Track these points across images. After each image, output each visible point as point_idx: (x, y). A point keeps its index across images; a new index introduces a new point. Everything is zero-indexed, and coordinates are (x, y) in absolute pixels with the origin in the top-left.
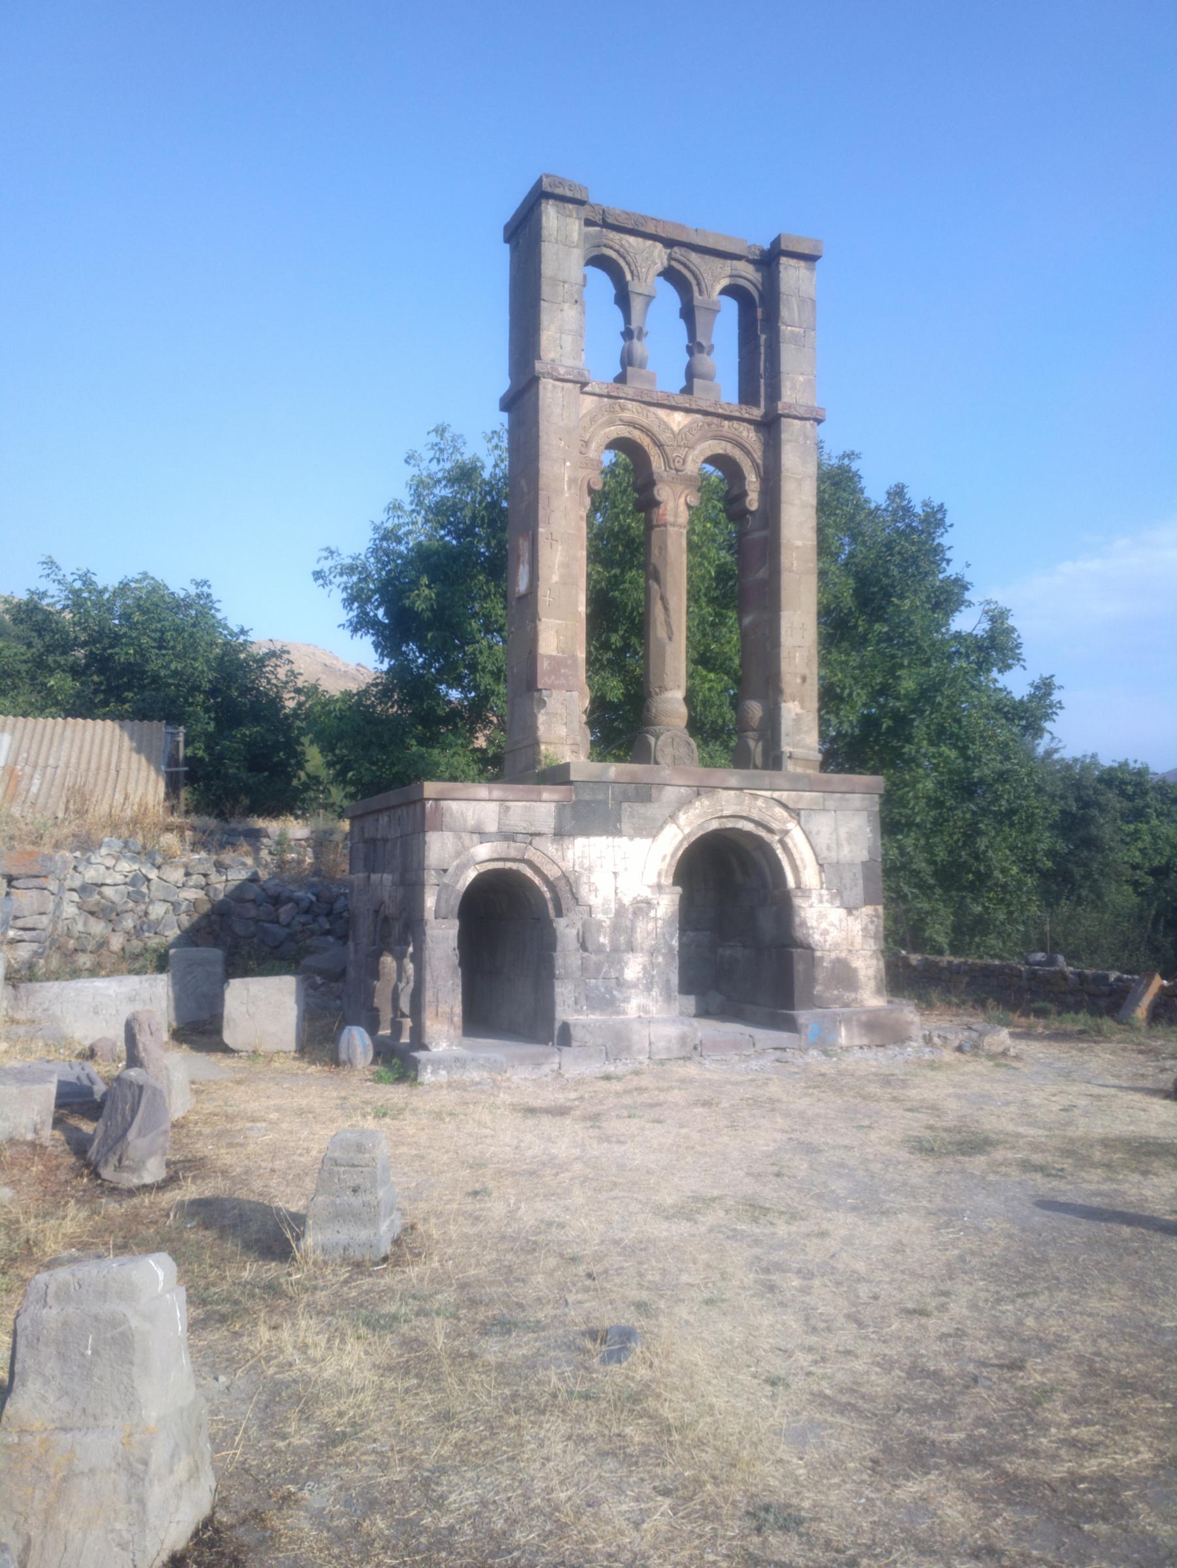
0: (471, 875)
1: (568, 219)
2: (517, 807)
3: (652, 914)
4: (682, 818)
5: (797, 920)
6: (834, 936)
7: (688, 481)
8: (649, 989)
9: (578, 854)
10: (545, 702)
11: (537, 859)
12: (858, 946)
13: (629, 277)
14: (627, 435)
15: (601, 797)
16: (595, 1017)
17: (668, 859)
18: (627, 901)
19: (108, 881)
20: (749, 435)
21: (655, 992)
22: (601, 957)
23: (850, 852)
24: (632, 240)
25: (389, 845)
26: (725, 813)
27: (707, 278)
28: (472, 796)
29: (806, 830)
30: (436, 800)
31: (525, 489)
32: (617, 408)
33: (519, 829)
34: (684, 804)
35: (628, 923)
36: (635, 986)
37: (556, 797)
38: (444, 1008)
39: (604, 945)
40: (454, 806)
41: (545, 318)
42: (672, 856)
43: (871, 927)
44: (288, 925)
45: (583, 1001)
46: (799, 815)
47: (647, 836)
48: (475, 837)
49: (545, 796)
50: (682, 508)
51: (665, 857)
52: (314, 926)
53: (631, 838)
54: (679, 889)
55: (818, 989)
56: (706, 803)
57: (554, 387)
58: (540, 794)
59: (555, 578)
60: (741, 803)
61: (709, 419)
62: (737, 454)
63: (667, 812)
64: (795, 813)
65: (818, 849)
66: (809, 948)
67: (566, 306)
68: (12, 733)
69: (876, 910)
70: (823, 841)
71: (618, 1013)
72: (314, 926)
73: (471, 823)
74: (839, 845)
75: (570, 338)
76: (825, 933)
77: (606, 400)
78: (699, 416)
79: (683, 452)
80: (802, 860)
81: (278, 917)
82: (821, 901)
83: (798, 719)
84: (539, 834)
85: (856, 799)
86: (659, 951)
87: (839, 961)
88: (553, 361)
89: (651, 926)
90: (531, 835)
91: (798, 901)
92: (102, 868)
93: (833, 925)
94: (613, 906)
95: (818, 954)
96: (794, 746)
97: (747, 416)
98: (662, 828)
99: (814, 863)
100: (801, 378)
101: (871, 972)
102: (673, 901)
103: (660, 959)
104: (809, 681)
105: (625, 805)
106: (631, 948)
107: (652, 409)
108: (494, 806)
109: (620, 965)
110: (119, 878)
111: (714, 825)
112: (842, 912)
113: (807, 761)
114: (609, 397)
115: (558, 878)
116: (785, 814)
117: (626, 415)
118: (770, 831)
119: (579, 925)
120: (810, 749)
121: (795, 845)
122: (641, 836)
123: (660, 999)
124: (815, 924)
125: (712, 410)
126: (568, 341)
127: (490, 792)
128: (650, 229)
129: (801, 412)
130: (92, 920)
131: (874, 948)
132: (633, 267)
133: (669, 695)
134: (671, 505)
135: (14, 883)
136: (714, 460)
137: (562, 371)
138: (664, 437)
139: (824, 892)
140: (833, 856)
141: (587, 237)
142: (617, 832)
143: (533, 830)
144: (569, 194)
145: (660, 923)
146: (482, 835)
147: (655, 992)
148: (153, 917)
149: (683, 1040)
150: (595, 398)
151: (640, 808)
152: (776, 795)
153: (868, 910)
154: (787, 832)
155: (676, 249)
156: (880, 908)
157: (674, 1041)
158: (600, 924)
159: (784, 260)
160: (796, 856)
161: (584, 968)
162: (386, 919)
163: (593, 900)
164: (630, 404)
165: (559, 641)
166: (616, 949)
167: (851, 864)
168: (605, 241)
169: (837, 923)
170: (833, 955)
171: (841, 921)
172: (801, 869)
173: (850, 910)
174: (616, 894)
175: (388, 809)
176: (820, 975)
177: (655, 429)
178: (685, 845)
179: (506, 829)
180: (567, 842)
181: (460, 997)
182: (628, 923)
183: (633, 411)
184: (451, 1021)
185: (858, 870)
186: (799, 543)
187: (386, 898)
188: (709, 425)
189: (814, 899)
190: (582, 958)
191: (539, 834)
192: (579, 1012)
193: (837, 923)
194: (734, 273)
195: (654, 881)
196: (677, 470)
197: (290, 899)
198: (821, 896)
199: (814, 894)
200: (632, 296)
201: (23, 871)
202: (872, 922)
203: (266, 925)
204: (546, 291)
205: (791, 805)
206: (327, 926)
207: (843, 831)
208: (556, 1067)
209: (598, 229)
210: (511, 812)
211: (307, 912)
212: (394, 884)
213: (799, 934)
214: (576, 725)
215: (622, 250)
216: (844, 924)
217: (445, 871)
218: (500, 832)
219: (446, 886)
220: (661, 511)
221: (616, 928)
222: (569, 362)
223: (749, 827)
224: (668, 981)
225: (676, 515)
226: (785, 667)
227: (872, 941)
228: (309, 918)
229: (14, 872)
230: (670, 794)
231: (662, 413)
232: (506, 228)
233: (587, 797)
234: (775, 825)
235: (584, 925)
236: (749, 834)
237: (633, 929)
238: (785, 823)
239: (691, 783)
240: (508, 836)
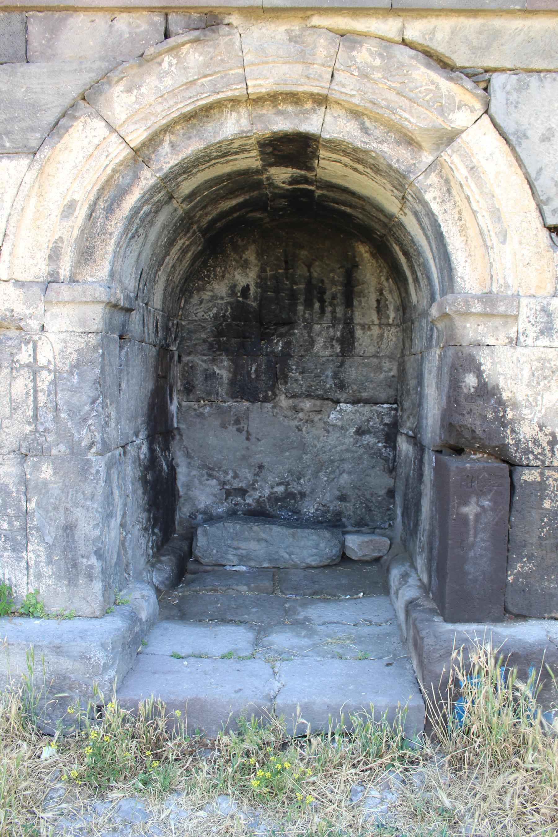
4: (120, 102)
17: (82, 212)
21: (35, 552)
26: (260, 85)
29: (509, 127)
51: (70, 208)
56: (194, 57)
60: (303, 57)
63: (72, 86)
80: (496, 214)
86: (43, 452)
89: (21, 385)
98: (56, 129)
99: (537, 223)
102: (83, 321)
103: (47, 472)
123: (48, 570)
145: (46, 378)
147: (35, 552)
152: (416, 30)
160: (480, 203)
172: (494, 241)
195: (39, 268)
199: (527, 310)
205: (460, 59)
224: (69, 529)
234: (416, 120)
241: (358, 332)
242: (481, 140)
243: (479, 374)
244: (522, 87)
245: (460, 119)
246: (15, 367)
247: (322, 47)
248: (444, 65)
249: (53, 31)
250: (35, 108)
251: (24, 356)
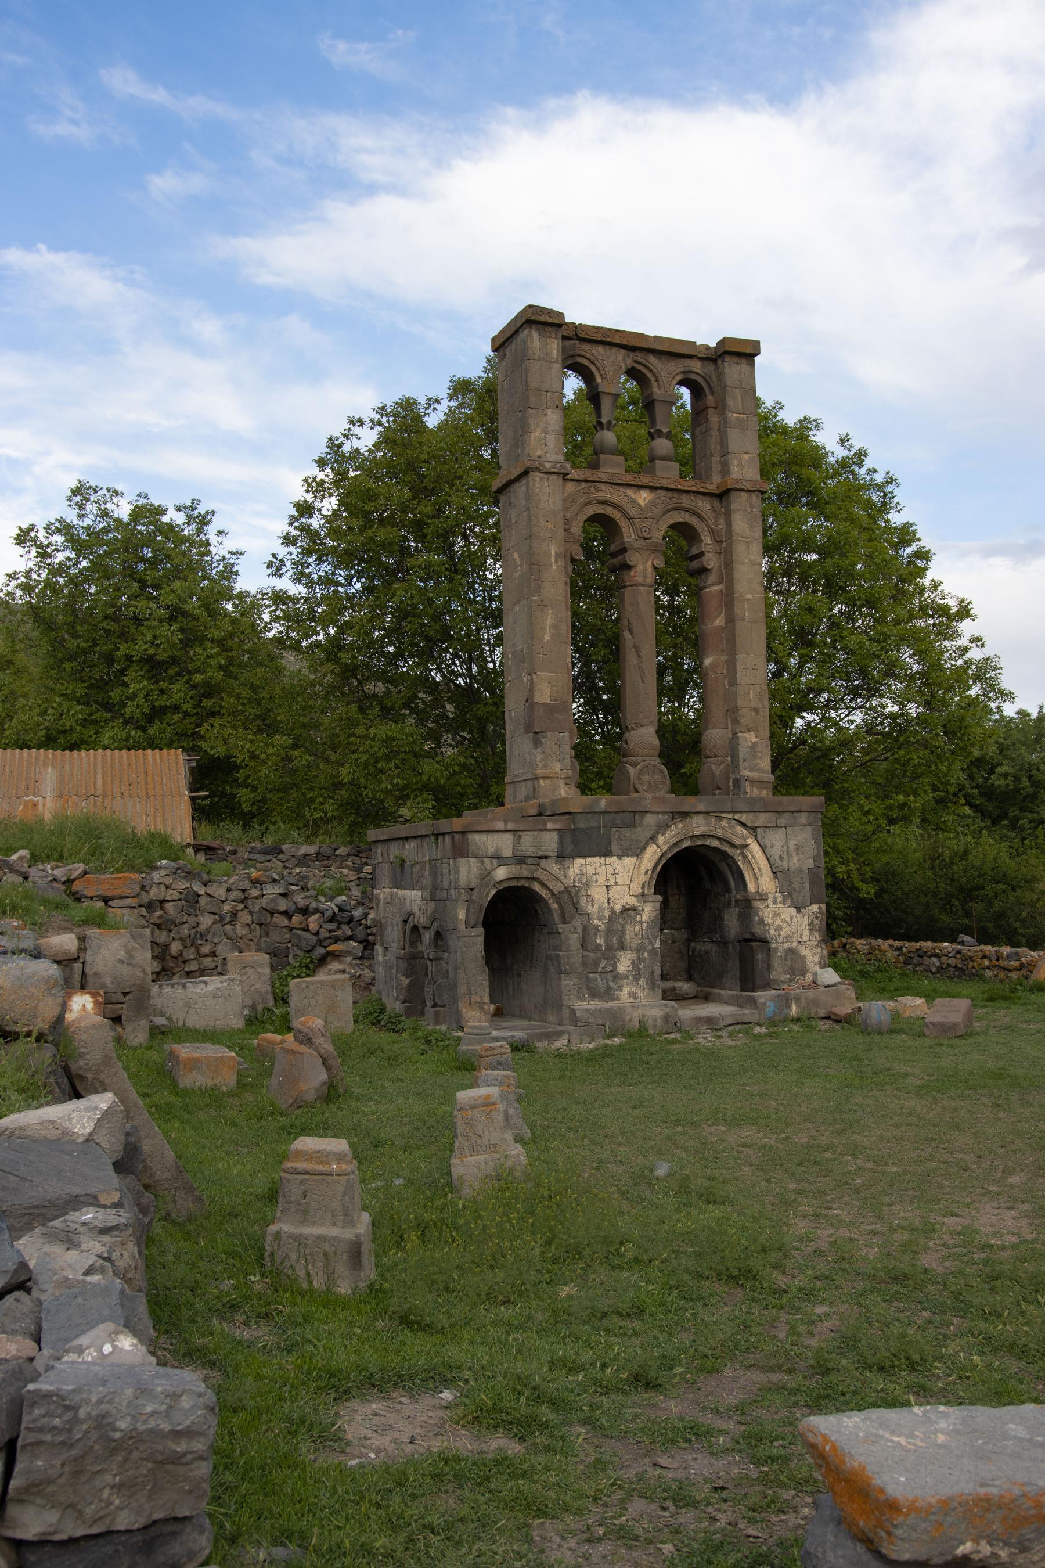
0: (493, 892)
1: (548, 340)
2: (527, 838)
3: (638, 919)
4: (661, 840)
5: (757, 918)
6: (786, 930)
7: (654, 549)
8: (637, 979)
9: (577, 871)
10: (541, 743)
11: (543, 878)
12: (805, 938)
13: (599, 380)
14: (602, 511)
15: (594, 824)
16: (595, 1004)
17: (650, 873)
18: (618, 908)
19: (168, 898)
20: (704, 505)
21: (642, 982)
22: (599, 955)
23: (799, 860)
24: (600, 349)
25: (417, 868)
26: (695, 833)
27: (664, 376)
28: (491, 829)
30: (463, 833)
31: (518, 562)
32: (593, 490)
33: (529, 854)
34: (662, 828)
35: (619, 927)
36: (626, 977)
37: (558, 826)
38: (476, 998)
39: (600, 945)
40: (477, 837)
41: (532, 422)
42: (654, 870)
43: (817, 922)
44: (317, 934)
45: (585, 991)
47: (632, 856)
48: (495, 861)
49: (550, 826)
50: (650, 570)
51: (647, 872)
52: (338, 933)
53: (620, 858)
54: (659, 898)
55: (774, 975)
56: (680, 825)
57: (541, 478)
58: (545, 824)
59: (547, 638)
60: (708, 825)
61: (670, 494)
62: (694, 521)
63: (648, 835)
64: (754, 829)
65: (772, 859)
66: (765, 942)
67: (549, 411)
68: (54, 767)
69: (820, 908)
70: (776, 852)
71: (613, 1000)
72: (338, 933)
73: (491, 850)
74: (789, 856)
75: (553, 437)
76: (779, 928)
77: (583, 485)
78: (662, 493)
79: (649, 522)
80: (759, 869)
81: (307, 925)
82: (775, 903)
83: (754, 746)
84: (546, 857)
85: (803, 818)
87: (791, 951)
88: (539, 457)
89: (637, 928)
90: (540, 858)
91: (756, 904)
92: (163, 888)
93: (784, 921)
94: (606, 913)
95: (774, 946)
96: (752, 770)
97: (702, 490)
98: (644, 848)
100: (746, 456)
101: (816, 959)
103: (646, 955)
105: (614, 830)
106: (622, 948)
107: (621, 489)
108: (509, 837)
109: (614, 961)
110: (176, 895)
111: (687, 843)
112: (793, 911)
113: (760, 783)
114: (586, 481)
115: (562, 892)
116: (745, 832)
117: (600, 496)
118: (733, 846)
119: (580, 930)
120: (764, 771)
121: (753, 856)
124: (770, 921)
125: (672, 486)
126: (552, 440)
127: (505, 825)
128: (617, 340)
129: (749, 486)
130: (157, 932)
131: (818, 939)
132: (602, 372)
133: (644, 730)
134: (640, 567)
135: (110, 903)
136: (673, 527)
137: (548, 465)
138: (633, 512)
139: (778, 895)
140: (785, 864)
141: (564, 349)
142: (608, 854)
143: (541, 854)
144: (550, 320)
146: (500, 860)
147: (642, 982)
148: (203, 927)
149: (666, 1018)
150: (574, 483)
151: (627, 833)
152: (737, 817)
153: (815, 908)
154: (746, 846)
155: (637, 353)
156: (823, 906)
157: (659, 1020)
158: (596, 928)
159: (727, 358)
160: (755, 866)
161: (584, 964)
162: (415, 928)
163: (589, 909)
164: (603, 488)
165: (552, 692)
166: (609, 948)
167: (800, 870)
168: (579, 352)
169: (788, 919)
170: (786, 946)
171: (791, 918)
173: (799, 909)
174: (609, 903)
175: (415, 837)
176: (776, 963)
177: (626, 506)
178: (664, 861)
179: (518, 854)
180: (567, 862)
181: (488, 990)
182: (619, 927)
183: (606, 493)
184: (482, 1009)
185: (806, 876)
186: (750, 596)
187: (416, 909)
188: (670, 499)
189: (770, 902)
190: (583, 956)
191: (546, 857)
192: (580, 999)
193: (788, 919)
194: (687, 369)
195: (640, 891)
196: (645, 539)
197: (317, 910)
198: (775, 898)
200: (601, 395)
201: (117, 892)
202: (817, 918)
203: (299, 932)
204: (532, 399)
206: (350, 933)
207: (792, 844)
208: (565, 1042)
209: (572, 342)
210: (522, 840)
211: (331, 920)
212: (423, 899)
213: (758, 930)
214: (568, 761)
215: (592, 358)
216: (794, 920)
217: (472, 889)
218: (514, 856)
219: (474, 902)
220: (632, 574)
221: (609, 931)
222: (553, 458)
223: (715, 843)
224: (653, 972)
225: (645, 577)
226: (740, 702)
227: (817, 934)
228: (333, 926)
229: (109, 894)
230: (650, 820)
231: (630, 492)
232: (493, 339)
233: (582, 825)
234: (737, 842)
235: (585, 929)
236: (715, 849)
237: (623, 932)
238: (745, 839)
239: (668, 810)
240: (520, 860)
241: (670, 898)
242: (755, 847)
243: (758, 915)
244: (765, 832)
245: (749, 841)
246: (636, 922)
247: (713, 821)
248: (744, 825)
249: (642, 818)
250: (638, 841)
251: (638, 919)
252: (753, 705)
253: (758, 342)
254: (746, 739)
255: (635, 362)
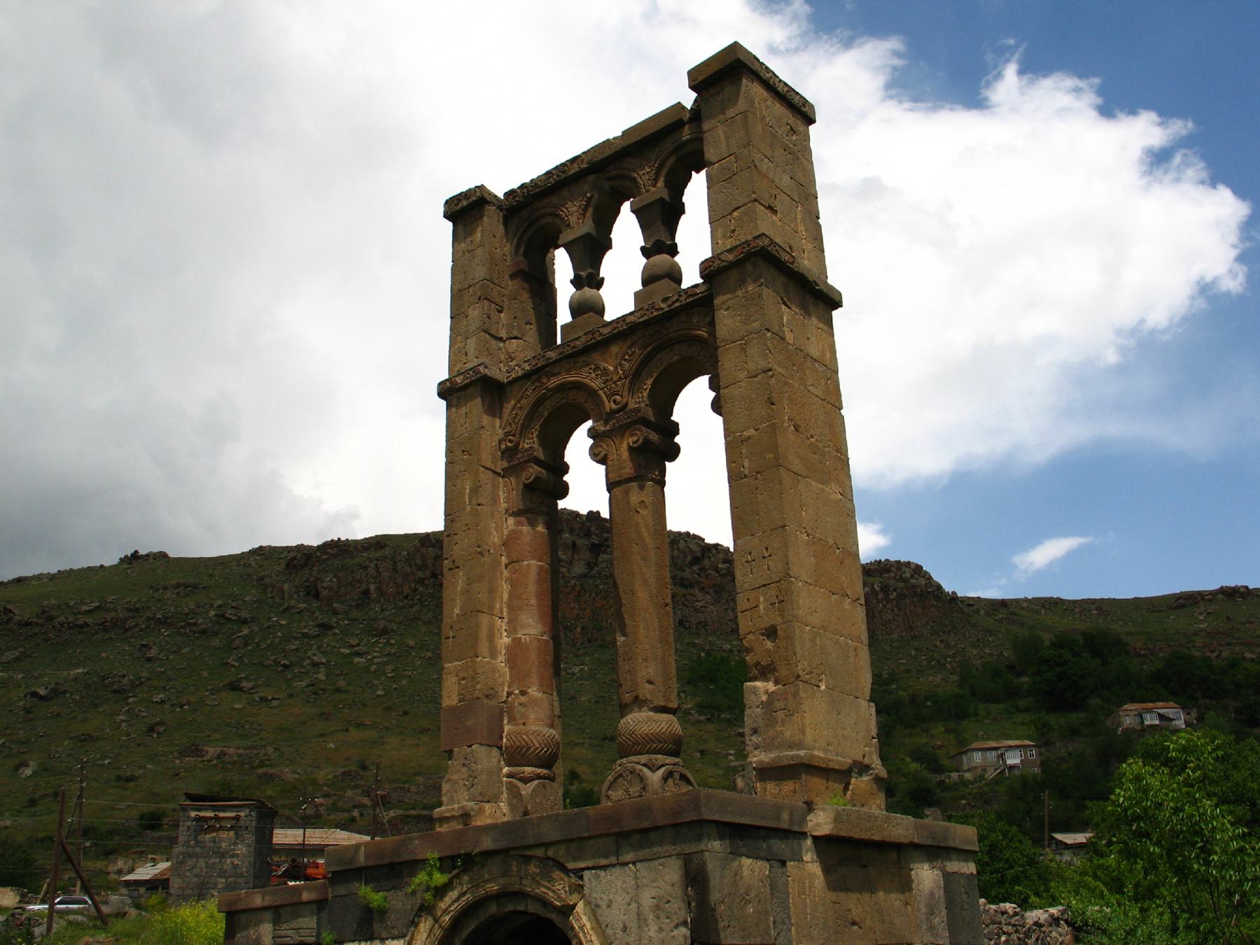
23: (661, 930)
28: (249, 906)
46: (581, 878)
57: (459, 398)
59: (457, 611)
96: (768, 747)
100: (735, 214)
104: (780, 633)
107: (582, 359)
122: (393, 939)
126: (472, 344)
128: (575, 169)
207: (647, 898)
252: (767, 622)
253: (735, 47)
254: (755, 691)
255: (610, 179)
